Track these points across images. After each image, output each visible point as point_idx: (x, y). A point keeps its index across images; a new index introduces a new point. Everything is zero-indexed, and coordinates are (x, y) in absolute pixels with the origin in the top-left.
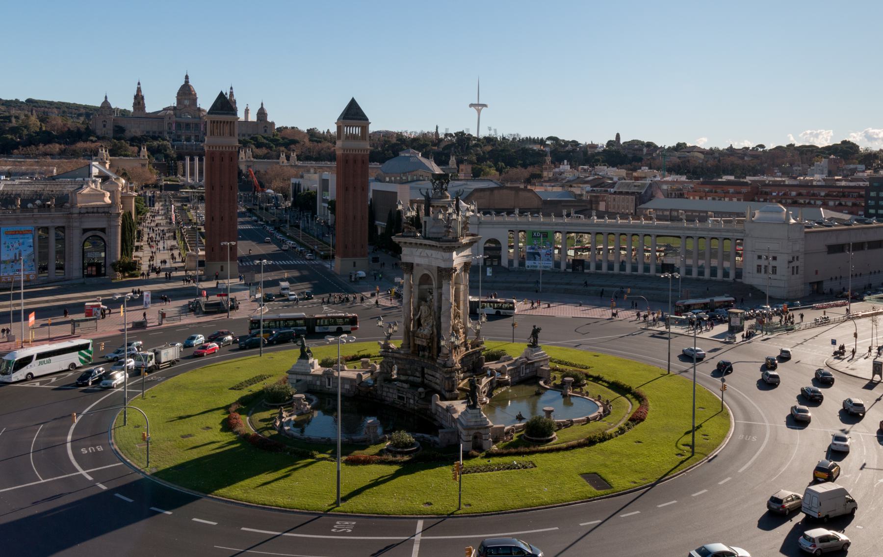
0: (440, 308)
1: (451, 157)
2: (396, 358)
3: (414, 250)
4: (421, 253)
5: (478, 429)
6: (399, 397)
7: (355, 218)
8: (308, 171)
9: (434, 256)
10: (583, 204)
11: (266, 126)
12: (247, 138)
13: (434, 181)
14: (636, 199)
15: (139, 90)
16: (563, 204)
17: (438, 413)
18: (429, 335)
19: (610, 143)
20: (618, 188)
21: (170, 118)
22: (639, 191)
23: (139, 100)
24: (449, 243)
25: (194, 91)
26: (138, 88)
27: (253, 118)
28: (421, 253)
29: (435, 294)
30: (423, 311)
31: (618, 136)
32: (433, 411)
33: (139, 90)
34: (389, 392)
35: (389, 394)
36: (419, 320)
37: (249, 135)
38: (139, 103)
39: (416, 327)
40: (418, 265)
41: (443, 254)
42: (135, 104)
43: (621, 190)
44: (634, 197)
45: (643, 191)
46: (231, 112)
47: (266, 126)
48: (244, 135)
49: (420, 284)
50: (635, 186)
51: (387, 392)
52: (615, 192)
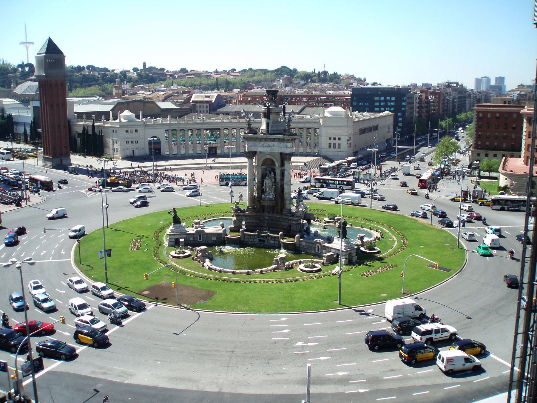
0: (282, 179)
3: (257, 143)
4: (263, 145)
6: (260, 240)
7: (59, 127)
10: (186, 110)
14: (209, 105)
16: (174, 111)
17: (301, 246)
19: (135, 70)
20: (195, 98)
22: (210, 100)
24: (293, 136)
28: (263, 145)
29: (278, 172)
30: (267, 183)
31: (144, 64)
32: (298, 246)
34: (250, 238)
35: (250, 240)
40: (260, 152)
41: (286, 144)
43: (197, 100)
44: (208, 105)
45: (213, 100)
49: (262, 165)
50: (206, 97)
51: (248, 238)
52: (193, 101)
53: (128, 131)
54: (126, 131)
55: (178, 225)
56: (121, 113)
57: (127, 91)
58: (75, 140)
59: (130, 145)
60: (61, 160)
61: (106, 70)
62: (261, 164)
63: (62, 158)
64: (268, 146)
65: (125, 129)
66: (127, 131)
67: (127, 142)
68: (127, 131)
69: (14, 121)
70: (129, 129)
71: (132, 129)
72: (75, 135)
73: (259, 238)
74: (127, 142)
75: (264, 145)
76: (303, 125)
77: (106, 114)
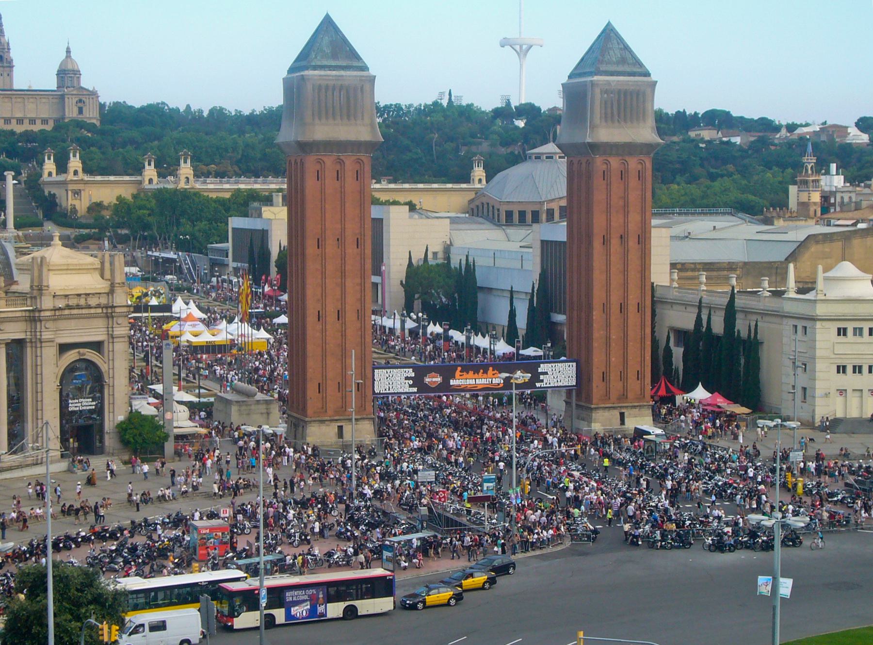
1: (475, 165)
8: (268, 200)
11: (80, 101)
12: (49, 127)
27: (51, 83)
37: (45, 121)
47: (80, 101)
48: (32, 121)
53: (845, 330)
54: (839, 329)
56: (825, 271)
57: (838, 196)
58: (668, 352)
59: (850, 380)
60: (622, 415)
61: (766, 126)
63: (626, 414)
65: (834, 327)
66: (842, 332)
67: (842, 369)
68: (842, 332)
69: (479, 284)
70: (850, 326)
71: (858, 325)
74: (838, 367)
77: (777, 270)
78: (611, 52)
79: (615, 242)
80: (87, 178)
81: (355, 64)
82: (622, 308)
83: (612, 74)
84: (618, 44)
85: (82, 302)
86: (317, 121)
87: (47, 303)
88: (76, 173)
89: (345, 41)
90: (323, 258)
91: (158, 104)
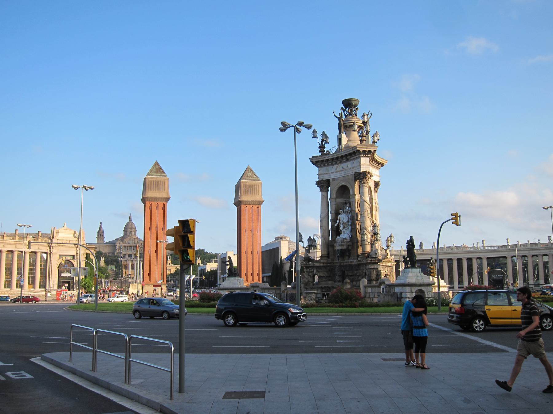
2: (317, 267)
4: (336, 169)
5: (420, 285)
9: (350, 166)
13: (345, 108)
15: (101, 227)
18: (348, 238)
21: (119, 244)
23: (100, 234)
25: (135, 226)
26: (100, 226)
28: (336, 169)
32: (362, 294)
33: (101, 227)
36: (338, 226)
38: (101, 235)
39: (334, 237)
40: (334, 180)
42: (98, 235)
46: (163, 174)
55: (232, 278)
62: (334, 196)
64: (342, 169)
72: (285, 273)
73: (322, 291)
75: (338, 170)
76: (538, 251)
78: (248, 174)
79: (249, 232)
80: (173, 265)
81: (163, 174)
82: (252, 253)
83: (247, 180)
84: (251, 171)
85: (68, 242)
86: (150, 191)
87: (55, 241)
88: (169, 264)
89: (161, 168)
90: (151, 233)
91: (210, 253)
